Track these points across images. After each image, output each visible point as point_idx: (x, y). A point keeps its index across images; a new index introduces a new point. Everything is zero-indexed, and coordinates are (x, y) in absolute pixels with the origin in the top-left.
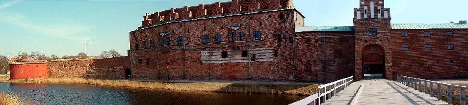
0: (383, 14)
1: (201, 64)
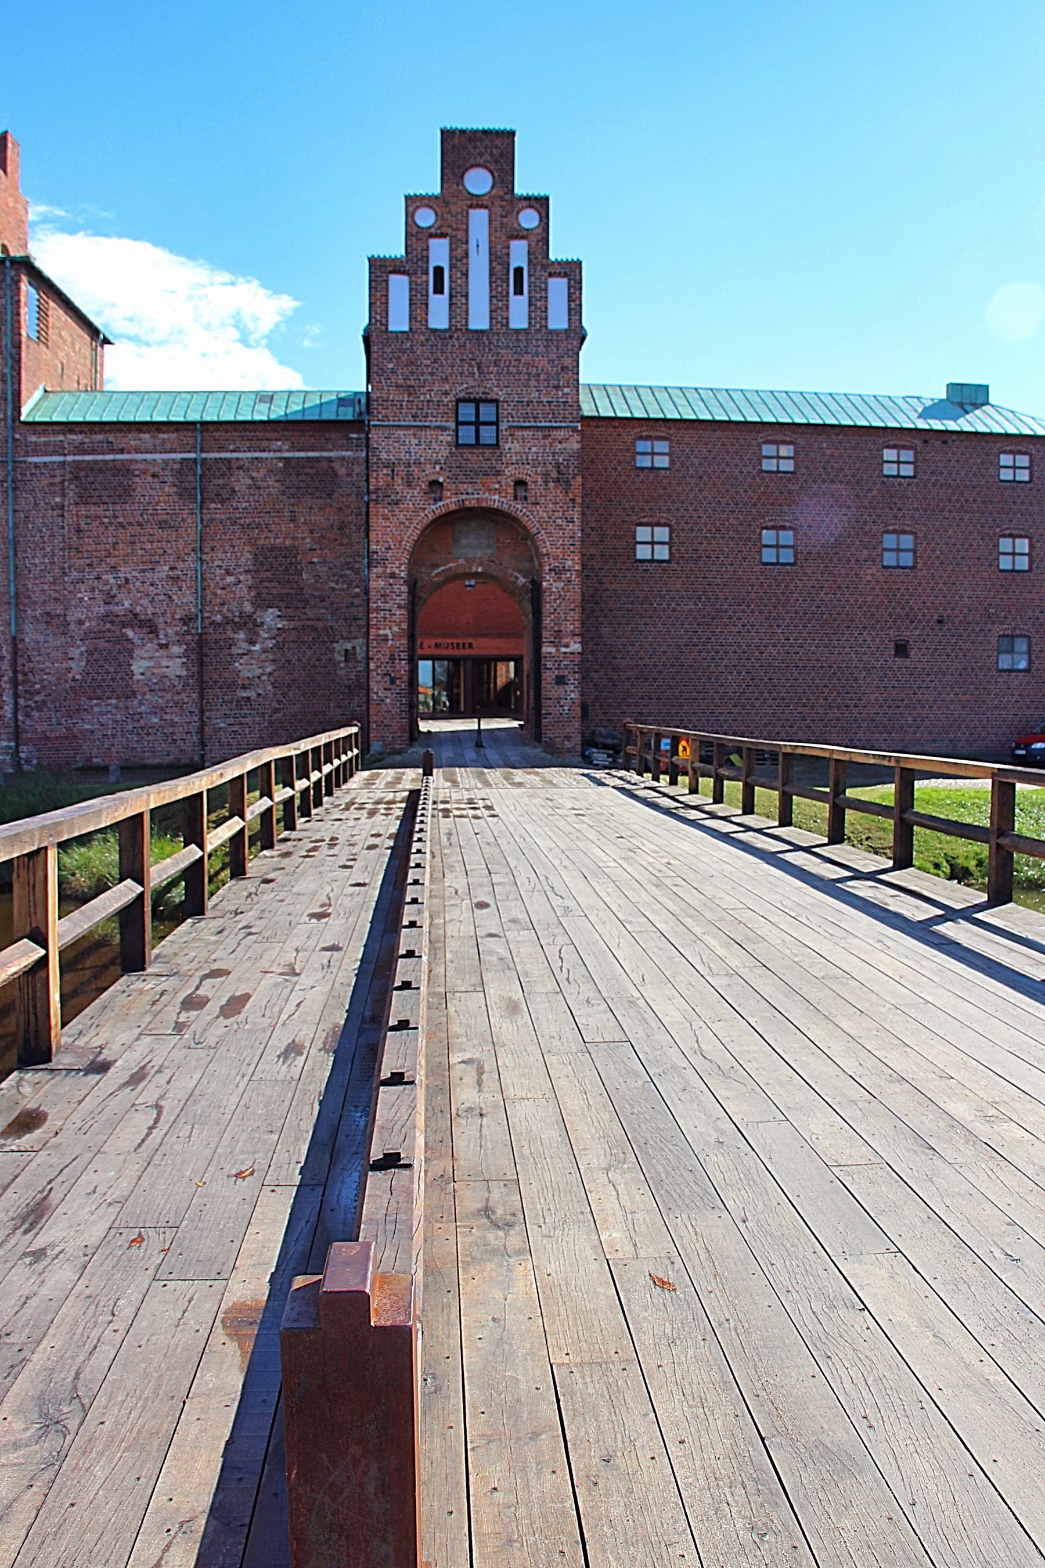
0: (538, 308)
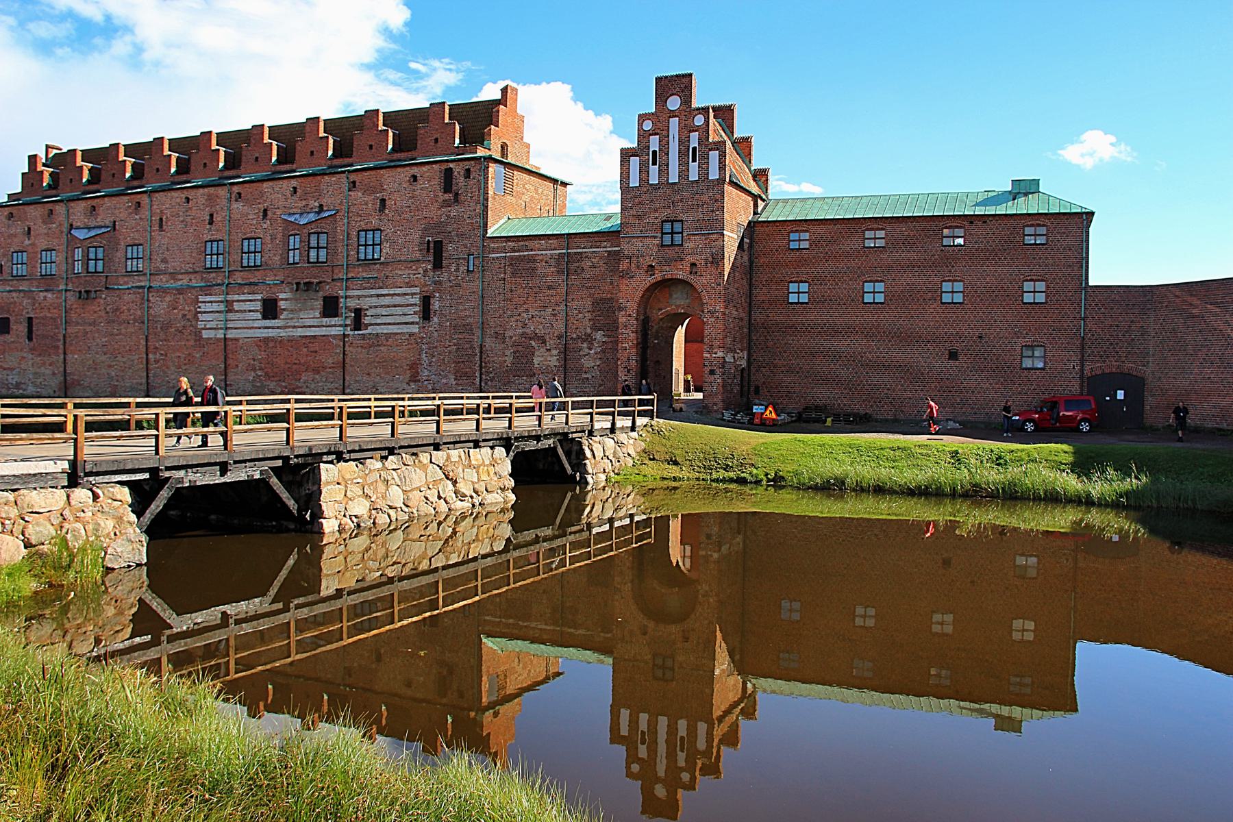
0: (704, 170)
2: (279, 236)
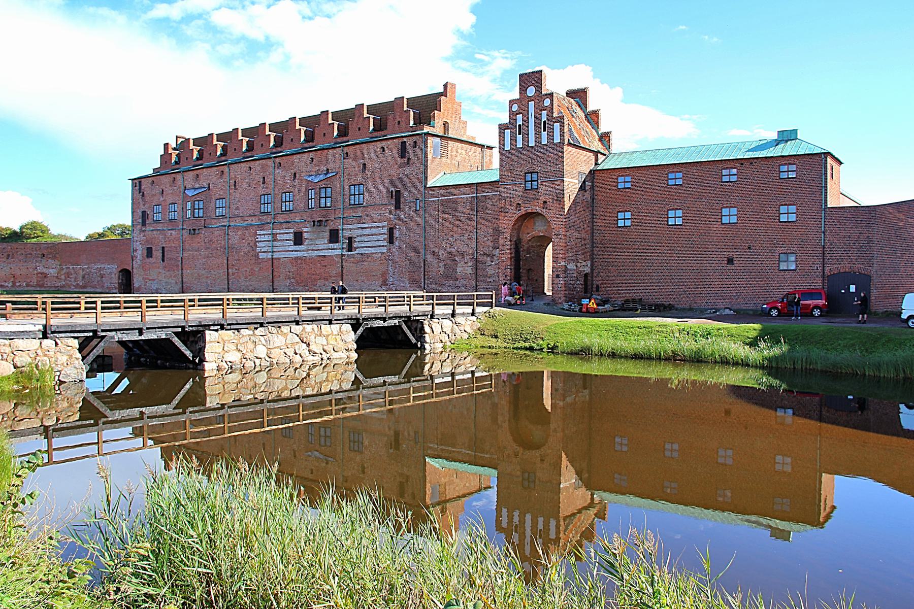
0: (551, 137)
1: (257, 255)
2: (303, 190)
